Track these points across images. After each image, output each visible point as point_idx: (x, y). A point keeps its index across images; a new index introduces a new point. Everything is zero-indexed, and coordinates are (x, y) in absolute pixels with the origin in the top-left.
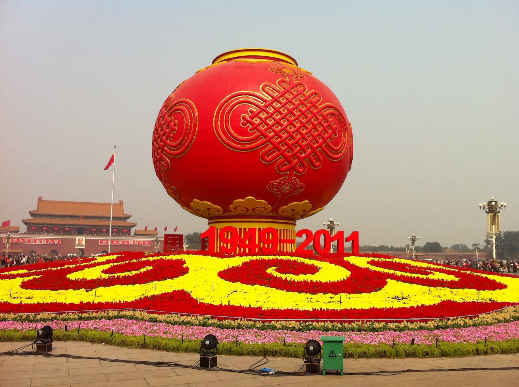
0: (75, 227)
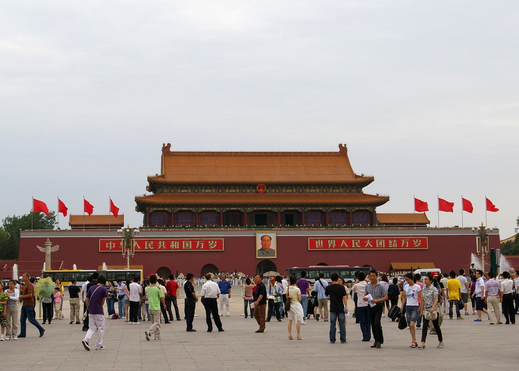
0: (249, 209)
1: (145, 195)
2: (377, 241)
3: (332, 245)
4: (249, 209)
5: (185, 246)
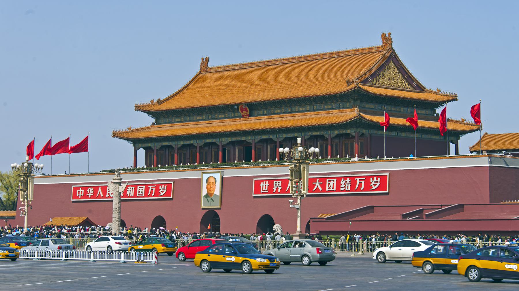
0: (225, 141)
1: (129, 129)
2: (328, 180)
3: (277, 188)
4: (224, 139)
5: (139, 192)
